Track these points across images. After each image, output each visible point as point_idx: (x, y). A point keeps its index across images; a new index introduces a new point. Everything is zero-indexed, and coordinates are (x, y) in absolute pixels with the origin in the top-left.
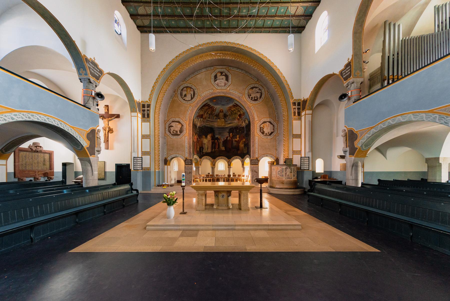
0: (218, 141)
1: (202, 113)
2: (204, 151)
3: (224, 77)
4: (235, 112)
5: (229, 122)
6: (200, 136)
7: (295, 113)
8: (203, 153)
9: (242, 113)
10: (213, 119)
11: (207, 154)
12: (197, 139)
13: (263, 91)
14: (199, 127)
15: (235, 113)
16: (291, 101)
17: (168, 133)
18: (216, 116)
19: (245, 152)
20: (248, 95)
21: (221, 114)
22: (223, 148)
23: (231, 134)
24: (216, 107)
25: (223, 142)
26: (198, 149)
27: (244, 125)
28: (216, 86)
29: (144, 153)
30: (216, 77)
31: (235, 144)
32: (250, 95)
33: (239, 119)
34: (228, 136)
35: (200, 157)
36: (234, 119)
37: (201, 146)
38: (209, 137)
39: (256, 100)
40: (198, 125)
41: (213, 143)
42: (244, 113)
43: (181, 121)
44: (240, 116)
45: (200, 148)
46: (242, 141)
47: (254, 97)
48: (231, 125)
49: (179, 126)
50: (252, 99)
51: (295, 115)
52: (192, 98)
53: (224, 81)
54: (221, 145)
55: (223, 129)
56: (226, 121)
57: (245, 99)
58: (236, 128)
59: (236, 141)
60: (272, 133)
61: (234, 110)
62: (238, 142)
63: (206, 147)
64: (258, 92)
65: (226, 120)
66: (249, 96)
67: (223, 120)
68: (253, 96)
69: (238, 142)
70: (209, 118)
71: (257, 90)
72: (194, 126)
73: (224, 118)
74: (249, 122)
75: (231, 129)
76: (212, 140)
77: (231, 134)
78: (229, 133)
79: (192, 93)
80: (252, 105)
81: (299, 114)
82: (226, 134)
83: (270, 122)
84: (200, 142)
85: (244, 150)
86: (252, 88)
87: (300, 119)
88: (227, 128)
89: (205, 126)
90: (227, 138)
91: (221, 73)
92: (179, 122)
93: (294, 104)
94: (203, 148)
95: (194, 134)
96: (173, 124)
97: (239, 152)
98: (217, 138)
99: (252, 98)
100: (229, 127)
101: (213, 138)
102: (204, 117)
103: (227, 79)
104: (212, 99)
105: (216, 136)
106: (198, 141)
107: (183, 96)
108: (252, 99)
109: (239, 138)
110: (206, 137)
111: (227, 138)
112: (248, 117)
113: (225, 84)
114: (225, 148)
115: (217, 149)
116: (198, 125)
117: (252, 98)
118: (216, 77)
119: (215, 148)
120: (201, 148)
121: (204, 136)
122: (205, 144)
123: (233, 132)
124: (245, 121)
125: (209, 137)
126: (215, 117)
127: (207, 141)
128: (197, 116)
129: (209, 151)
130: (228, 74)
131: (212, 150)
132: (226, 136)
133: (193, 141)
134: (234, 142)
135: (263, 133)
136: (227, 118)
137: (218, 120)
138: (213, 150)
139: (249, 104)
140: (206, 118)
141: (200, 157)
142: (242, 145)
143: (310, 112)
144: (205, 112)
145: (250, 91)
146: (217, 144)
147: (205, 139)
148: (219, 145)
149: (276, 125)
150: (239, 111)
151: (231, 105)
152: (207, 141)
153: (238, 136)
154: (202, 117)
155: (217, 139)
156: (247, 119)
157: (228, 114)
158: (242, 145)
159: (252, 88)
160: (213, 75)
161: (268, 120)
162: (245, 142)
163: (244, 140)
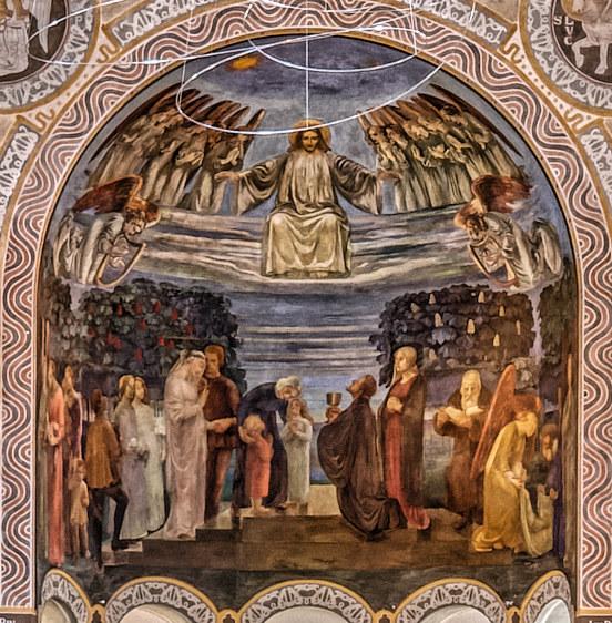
0: (271, 429)
1: (120, 167)
2: (134, 529)
4: (438, 152)
5: (385, 239)
6: (97, 389)
8: (119, 544)
9: (505, 172)
10: (229, 209)
11: (164, 557)
12: (73, 411)
14: (90, 301)
15: (447, 164)
18: (256, 181)
19: (537, 543)
20: (560, 32)
21: (309, 169)
22: (323, 500)
23: (404, 356)
24: (254, 104)
25: (326, 434)
26: (80, 516)
27: (527, 278)
31: (440, 456)
32: (579, 33)
33: (476, 221)
34: (375, 371)
36: (435, 215)
37: (104, 481)
38: (183, 383)
40: (85, 275)
41: (220, 444)
42: (523, 182)
44: (489, 189)
45: (98, 497)
46: (505, 433)
48: (405, 266)
50: (588, 69)
54: (302, 459)
56: (349, 233)
57: (528, 69)
58: (459, 300)
59: (448, 428)
61: (437, 140)
62: (471, 440)
63: (156, 486)
65: (356, 219)
67: (330, 219)
69: (471, 440)
70: (186, 204)
72: (55, 291)
73: (332, 205)
74: (569, 263)
75: (407, 302)
76: (212, 412)
77: (404, 356)
78: (388, 343)
80: (588, 118)
84: (96, 447)
85: (527, 517)
88: (363, 291)
89: (142, 282)
90: (366, 390)
94: (123, 503)
95: (49, 372)
97: (479, 539)
98: (267, 393)
99: (592, 54)
100: (388, 285)
101: (222, 396)
102: (137, 199)
104: (222, 63)
105: (255, 379)
106: (77, 440)
108: (588, 69)
109: (484, 398)
110: (156, 386)
111: (366, 390)
112: (555, 220)
114: (346, 494)
115: (255, 509)
116: (85, 275)
117: (592, 54)
119: (241, 501)
120: (110, 498)
121: (134, 384)
122: (142, 457)
123: (420, 337)
124: (534, 245)
125: (183, 383)
126: (245, 197)
127: (162, 429)
128: (80, 206)
129: (186, 521)
131: (211, 511)
132: (357, 376)
133: (43, 444)
134: (429, 435)
136: (368, 200)
137: (278, 219)
138: (226, 513)
139: (562, 107)
140: (153, 208)
142: (505, 477)
144: (150, 156)
146: (267, 452)
147: (141, 411)
148: (279, 462)
150: (481, 153)
151: (404, 94)
152: (162, 429)
153: (470, 380)
154: (119, 206)
155: (265, 400)
156: (555, 239)
157: (372, 165)
158: (505, 477)
162: (532, 443)
163: (527, 424)
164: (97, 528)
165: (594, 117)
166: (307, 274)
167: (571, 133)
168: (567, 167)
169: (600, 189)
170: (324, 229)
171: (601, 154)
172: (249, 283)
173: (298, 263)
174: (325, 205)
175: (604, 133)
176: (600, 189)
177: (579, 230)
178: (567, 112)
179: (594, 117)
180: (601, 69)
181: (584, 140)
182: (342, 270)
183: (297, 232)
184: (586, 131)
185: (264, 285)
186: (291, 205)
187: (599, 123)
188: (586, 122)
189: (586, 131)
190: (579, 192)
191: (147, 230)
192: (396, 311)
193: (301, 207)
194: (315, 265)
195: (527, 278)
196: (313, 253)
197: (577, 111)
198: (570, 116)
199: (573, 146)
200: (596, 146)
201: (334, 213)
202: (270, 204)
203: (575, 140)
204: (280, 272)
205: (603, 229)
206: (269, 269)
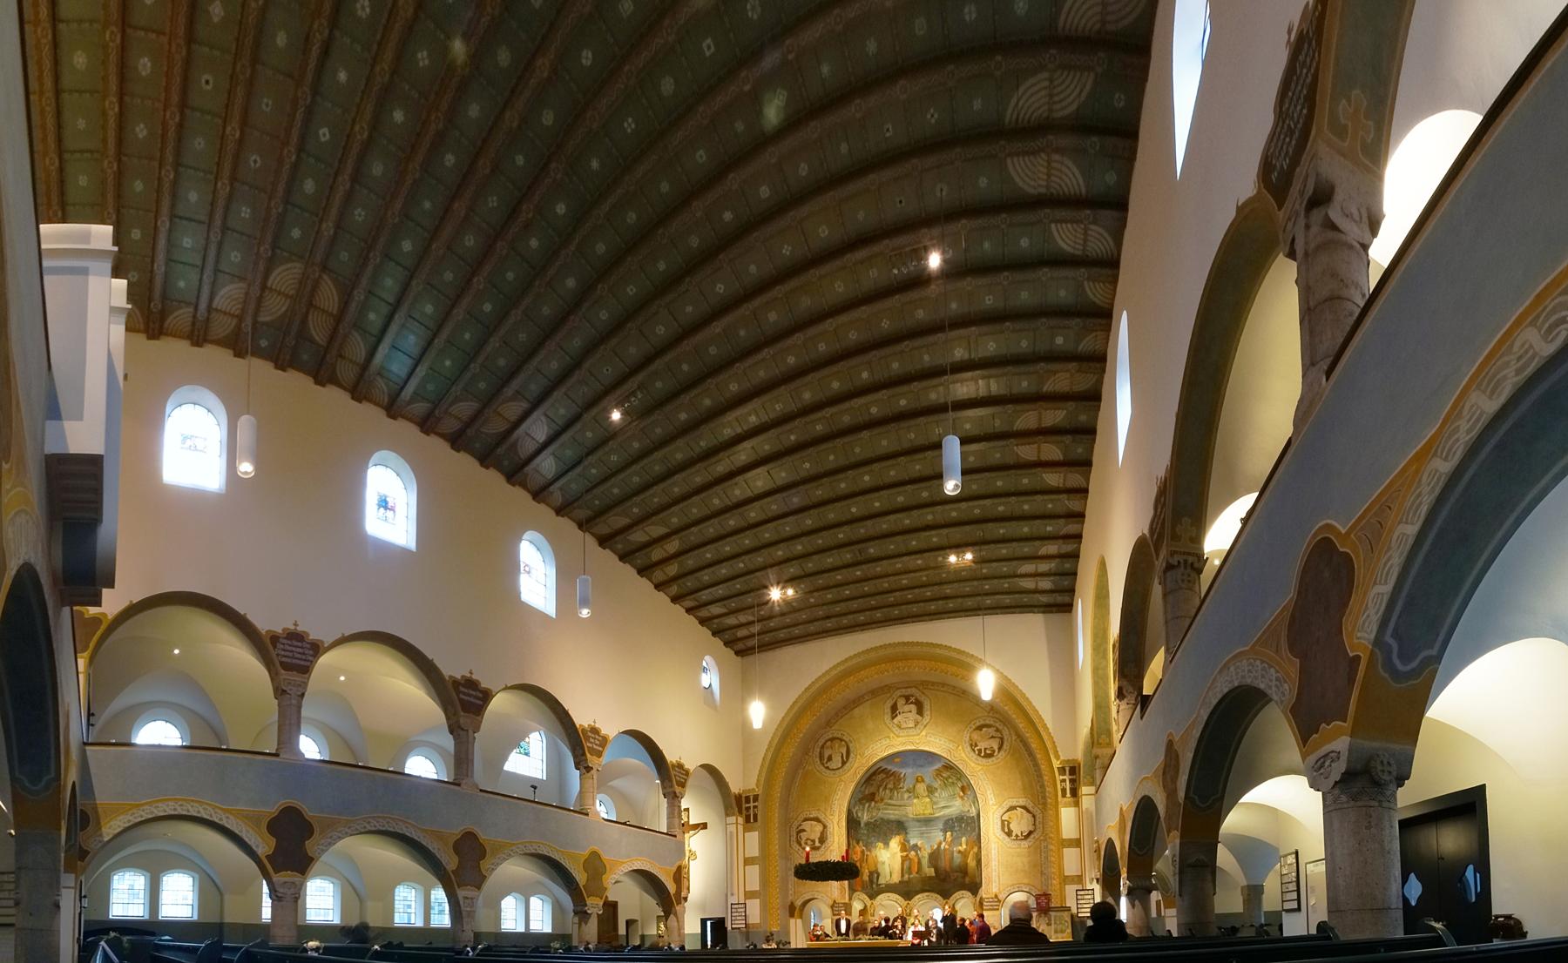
2: (882, 881)
3: (913, 707)
7: (1064, 790)
11: (890, 888)
13: (1006, 733)
16: (1056, 764)
17: (795, 845)
24: (903, 771)
25: (931, 855)
28: (895, 729)
29: (750, 895)
30: (894, 709)
35: (872, 897)
36: (953, 797)
39: (991, 756)
43: (822, 817)
44: (963, 789)
48: (947, 811)
49: (819, 828)
51: (1064, 795)
52: (844, 763)
53: (913, 715)
55: (927, 821)
60: (1030, 833)
66: (973, 745)
68: (982, 745)
69: (964, 854)
78: (945, 831)
79: (844, 751)
81: (1074, 793)
82: (939, 836)
83: (1024, 807)
86: (980, 728)
87: (1077, 804)
91: (907, 698)
92: (817, 820)
93: (1062, 770)
96: (806, 826)
97: (967, 880)
103: (920, 712)
107: (825, 760)
110: (887, 844)
113: (917, 723)
118: (894, 709)
125: (895, 843)
129: (896, 879)
130: (922, 699)
135: (1009, 834)
141: (872, 897)
143: (1092, 789)
145: (975, 736)
149: (1039, 815)
151: (938, 766)
159: (980, 728)
160: (889, 704)
161: (1022, 802)
164: (871, 881)
191: (881, 805)
192: (946, 823)
195: (973, 812)
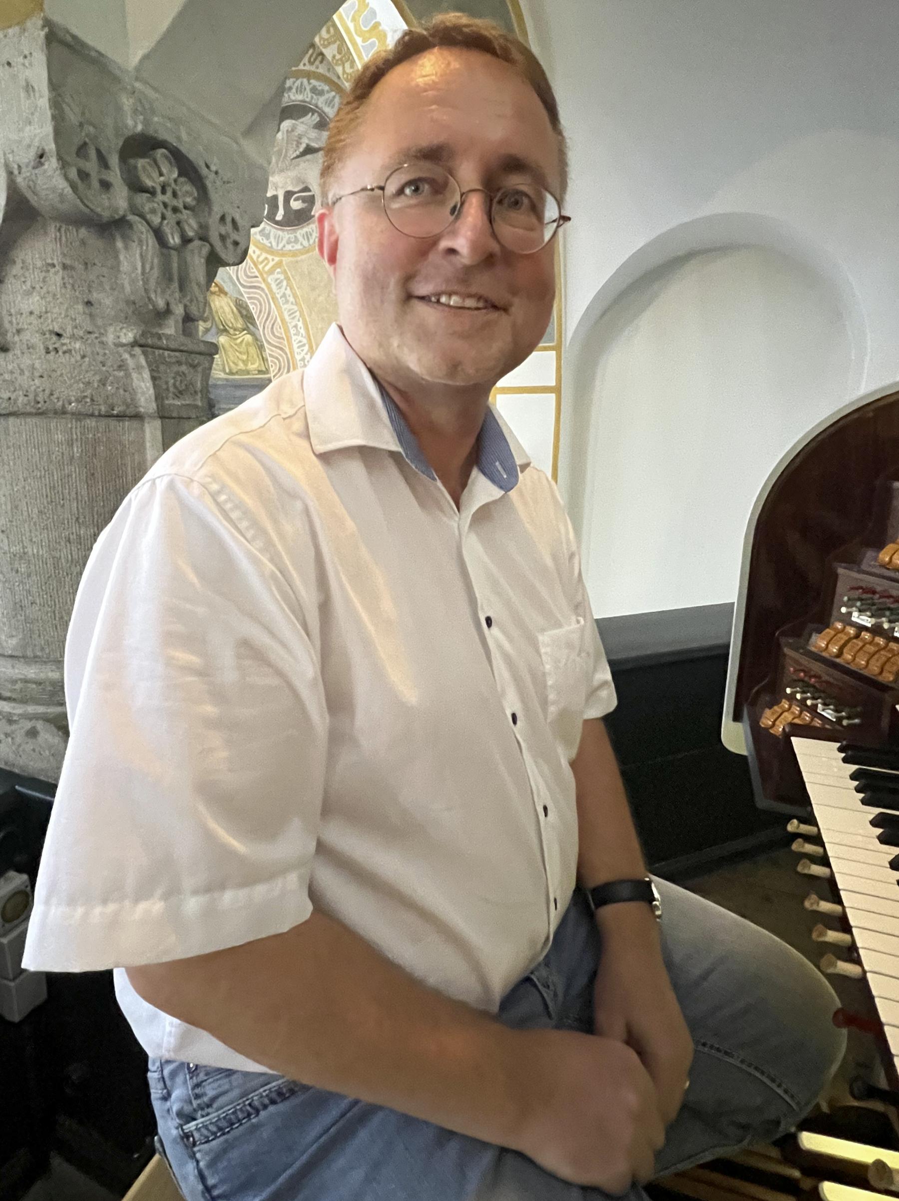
47: (288, 195)
64: (309, 150)
71: (304, 127)
165: (277, 259)
166: (248, 372)
167: (261, 274)
168: (261, 304)
169: (283, 320)
170: (248, 344)
171: (283, 290)
172: (219, 379)
173: (241, 366)
174: (244, 330)
175: (285, 272)
176: (283, 320)
177: (270, 355)
178: (258, 257)
179: (277, 259)
180: (279, 217)
181: (270, 279)
182: (264, 369)
183: (236, 347)
184: (271, 272)
185: (227, 380)
186: (225, 330)
187: (279, 264)
188: (271, 264)
189: (271, 272)
190: (269, 324)
193: (231, 331)
194: (251, 367)
196: (247, 360)
197: (264, 255)
198: (260, 259)
199: (263, 286)
200: (279, 284)
201: (248, 333)
202: (214, 330)
203: (264, 280)
204: (234, 371)
205: (286, 354)
206: (227, 371)
